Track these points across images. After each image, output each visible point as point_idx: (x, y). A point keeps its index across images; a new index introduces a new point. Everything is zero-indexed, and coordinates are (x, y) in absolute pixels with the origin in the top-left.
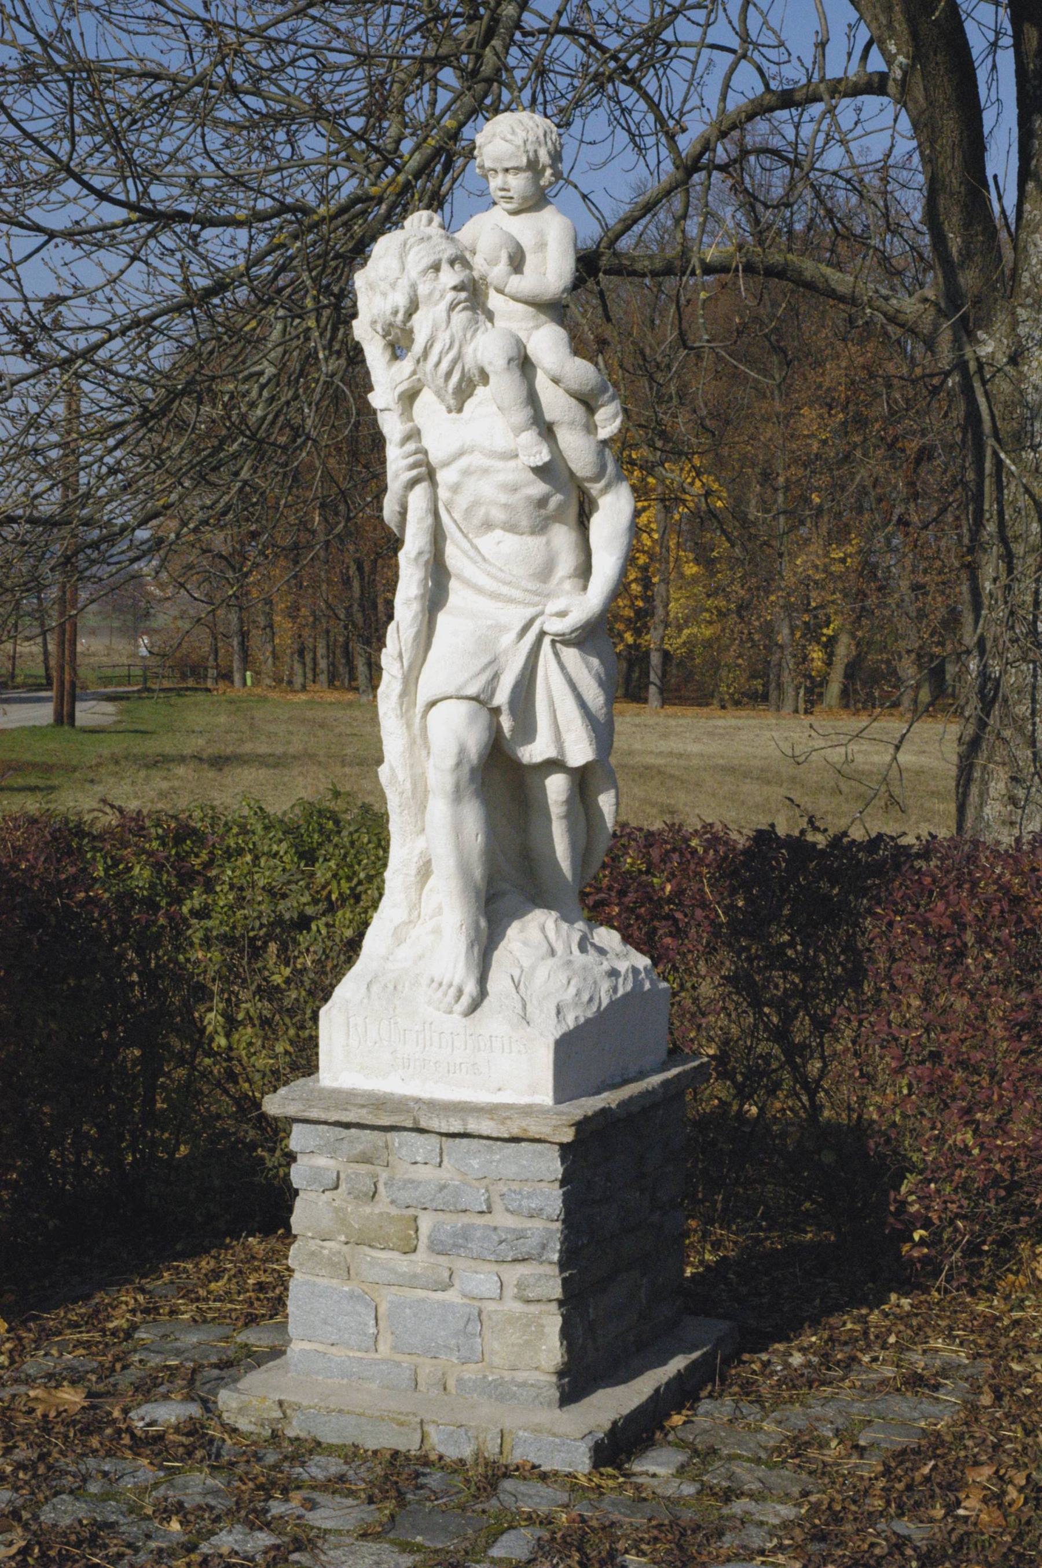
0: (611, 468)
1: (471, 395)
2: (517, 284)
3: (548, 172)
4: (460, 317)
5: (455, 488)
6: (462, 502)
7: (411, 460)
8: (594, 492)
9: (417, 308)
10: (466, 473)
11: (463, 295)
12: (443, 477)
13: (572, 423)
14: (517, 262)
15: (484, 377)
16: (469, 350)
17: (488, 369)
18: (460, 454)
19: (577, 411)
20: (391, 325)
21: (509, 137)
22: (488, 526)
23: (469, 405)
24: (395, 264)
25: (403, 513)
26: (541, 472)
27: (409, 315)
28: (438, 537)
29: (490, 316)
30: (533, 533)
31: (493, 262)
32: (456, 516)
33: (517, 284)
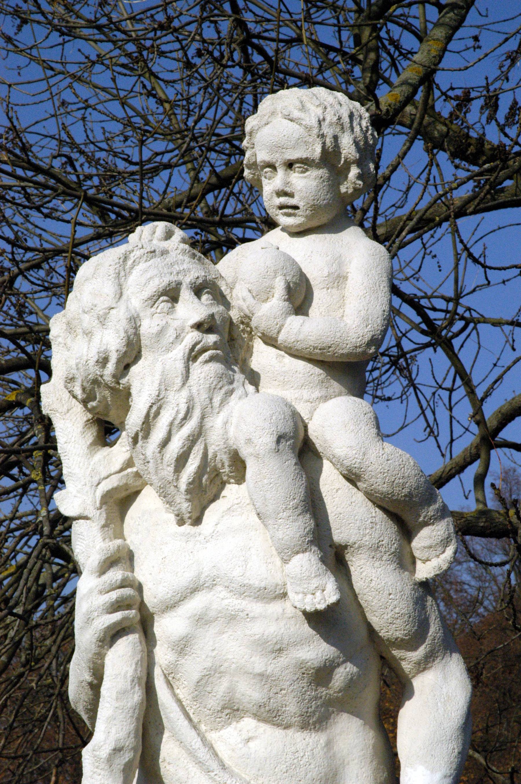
0: (434, 628)
1: (216, 497)
2: (298, 329)
3: (354, 171)
4: (204, 372)
5: (182, 646)
6: (192, 668)
7: (114, 595)
8: (406, 666)
9: (138, 357)
10: (201, 620)
11: (212, 338)
12: (166, 627)
13: (376, 547)
14: (299, 297)
15: (238, 466)
16: (216, 423)
17: (245, 452)
18: (194, 589)
19: (385, 530)
20: (95, 382)
21: (296, 114)
22: (232, 710)
23: (212, 513)
24: (109, 288)
25: (95, 688)
26: (322, 621)
27: (125, 365)
28: (149, 726)
29: (254, 378)
30: (304, 726)
31: (263, 295)
32: (181, 693)
33: (298, 329)
